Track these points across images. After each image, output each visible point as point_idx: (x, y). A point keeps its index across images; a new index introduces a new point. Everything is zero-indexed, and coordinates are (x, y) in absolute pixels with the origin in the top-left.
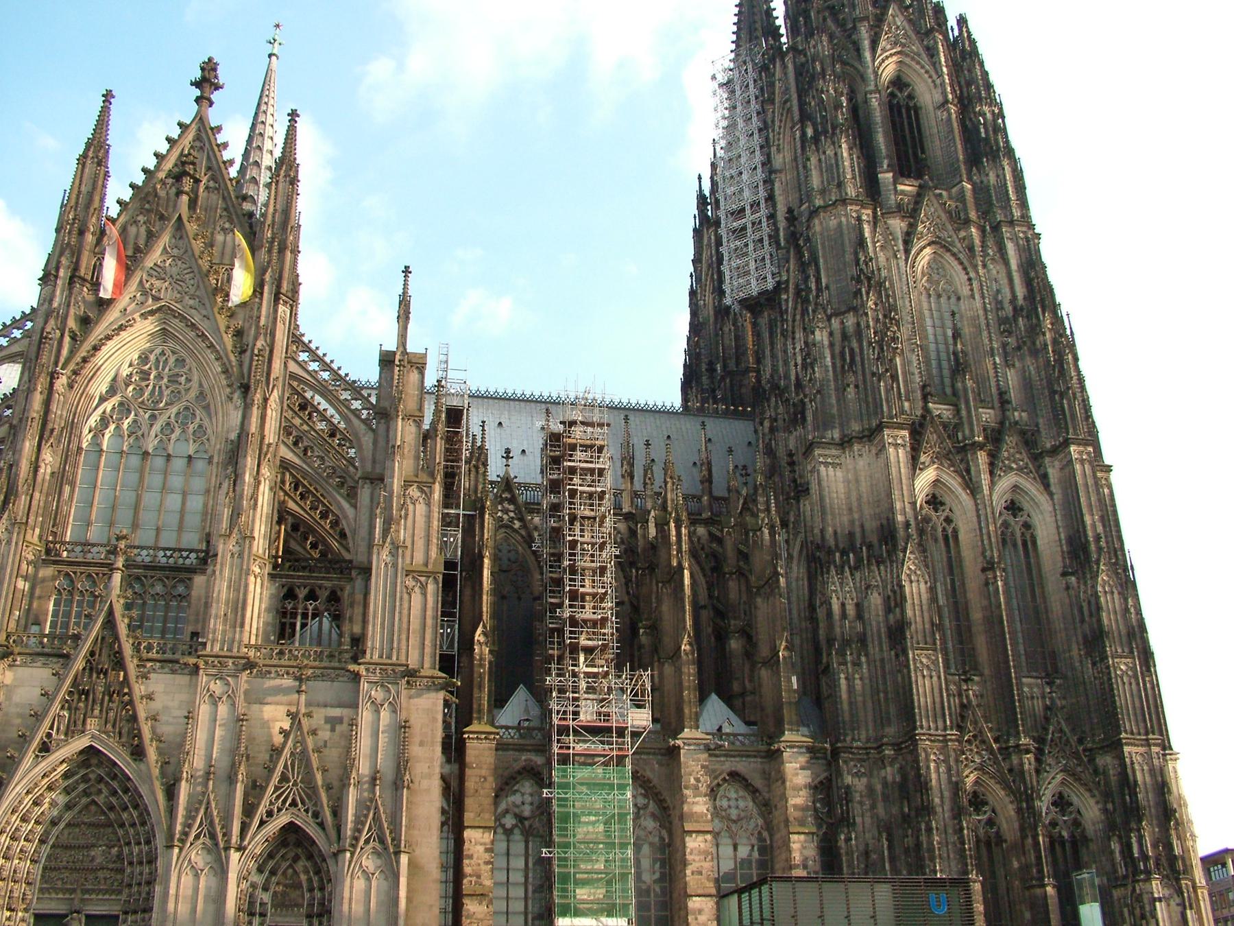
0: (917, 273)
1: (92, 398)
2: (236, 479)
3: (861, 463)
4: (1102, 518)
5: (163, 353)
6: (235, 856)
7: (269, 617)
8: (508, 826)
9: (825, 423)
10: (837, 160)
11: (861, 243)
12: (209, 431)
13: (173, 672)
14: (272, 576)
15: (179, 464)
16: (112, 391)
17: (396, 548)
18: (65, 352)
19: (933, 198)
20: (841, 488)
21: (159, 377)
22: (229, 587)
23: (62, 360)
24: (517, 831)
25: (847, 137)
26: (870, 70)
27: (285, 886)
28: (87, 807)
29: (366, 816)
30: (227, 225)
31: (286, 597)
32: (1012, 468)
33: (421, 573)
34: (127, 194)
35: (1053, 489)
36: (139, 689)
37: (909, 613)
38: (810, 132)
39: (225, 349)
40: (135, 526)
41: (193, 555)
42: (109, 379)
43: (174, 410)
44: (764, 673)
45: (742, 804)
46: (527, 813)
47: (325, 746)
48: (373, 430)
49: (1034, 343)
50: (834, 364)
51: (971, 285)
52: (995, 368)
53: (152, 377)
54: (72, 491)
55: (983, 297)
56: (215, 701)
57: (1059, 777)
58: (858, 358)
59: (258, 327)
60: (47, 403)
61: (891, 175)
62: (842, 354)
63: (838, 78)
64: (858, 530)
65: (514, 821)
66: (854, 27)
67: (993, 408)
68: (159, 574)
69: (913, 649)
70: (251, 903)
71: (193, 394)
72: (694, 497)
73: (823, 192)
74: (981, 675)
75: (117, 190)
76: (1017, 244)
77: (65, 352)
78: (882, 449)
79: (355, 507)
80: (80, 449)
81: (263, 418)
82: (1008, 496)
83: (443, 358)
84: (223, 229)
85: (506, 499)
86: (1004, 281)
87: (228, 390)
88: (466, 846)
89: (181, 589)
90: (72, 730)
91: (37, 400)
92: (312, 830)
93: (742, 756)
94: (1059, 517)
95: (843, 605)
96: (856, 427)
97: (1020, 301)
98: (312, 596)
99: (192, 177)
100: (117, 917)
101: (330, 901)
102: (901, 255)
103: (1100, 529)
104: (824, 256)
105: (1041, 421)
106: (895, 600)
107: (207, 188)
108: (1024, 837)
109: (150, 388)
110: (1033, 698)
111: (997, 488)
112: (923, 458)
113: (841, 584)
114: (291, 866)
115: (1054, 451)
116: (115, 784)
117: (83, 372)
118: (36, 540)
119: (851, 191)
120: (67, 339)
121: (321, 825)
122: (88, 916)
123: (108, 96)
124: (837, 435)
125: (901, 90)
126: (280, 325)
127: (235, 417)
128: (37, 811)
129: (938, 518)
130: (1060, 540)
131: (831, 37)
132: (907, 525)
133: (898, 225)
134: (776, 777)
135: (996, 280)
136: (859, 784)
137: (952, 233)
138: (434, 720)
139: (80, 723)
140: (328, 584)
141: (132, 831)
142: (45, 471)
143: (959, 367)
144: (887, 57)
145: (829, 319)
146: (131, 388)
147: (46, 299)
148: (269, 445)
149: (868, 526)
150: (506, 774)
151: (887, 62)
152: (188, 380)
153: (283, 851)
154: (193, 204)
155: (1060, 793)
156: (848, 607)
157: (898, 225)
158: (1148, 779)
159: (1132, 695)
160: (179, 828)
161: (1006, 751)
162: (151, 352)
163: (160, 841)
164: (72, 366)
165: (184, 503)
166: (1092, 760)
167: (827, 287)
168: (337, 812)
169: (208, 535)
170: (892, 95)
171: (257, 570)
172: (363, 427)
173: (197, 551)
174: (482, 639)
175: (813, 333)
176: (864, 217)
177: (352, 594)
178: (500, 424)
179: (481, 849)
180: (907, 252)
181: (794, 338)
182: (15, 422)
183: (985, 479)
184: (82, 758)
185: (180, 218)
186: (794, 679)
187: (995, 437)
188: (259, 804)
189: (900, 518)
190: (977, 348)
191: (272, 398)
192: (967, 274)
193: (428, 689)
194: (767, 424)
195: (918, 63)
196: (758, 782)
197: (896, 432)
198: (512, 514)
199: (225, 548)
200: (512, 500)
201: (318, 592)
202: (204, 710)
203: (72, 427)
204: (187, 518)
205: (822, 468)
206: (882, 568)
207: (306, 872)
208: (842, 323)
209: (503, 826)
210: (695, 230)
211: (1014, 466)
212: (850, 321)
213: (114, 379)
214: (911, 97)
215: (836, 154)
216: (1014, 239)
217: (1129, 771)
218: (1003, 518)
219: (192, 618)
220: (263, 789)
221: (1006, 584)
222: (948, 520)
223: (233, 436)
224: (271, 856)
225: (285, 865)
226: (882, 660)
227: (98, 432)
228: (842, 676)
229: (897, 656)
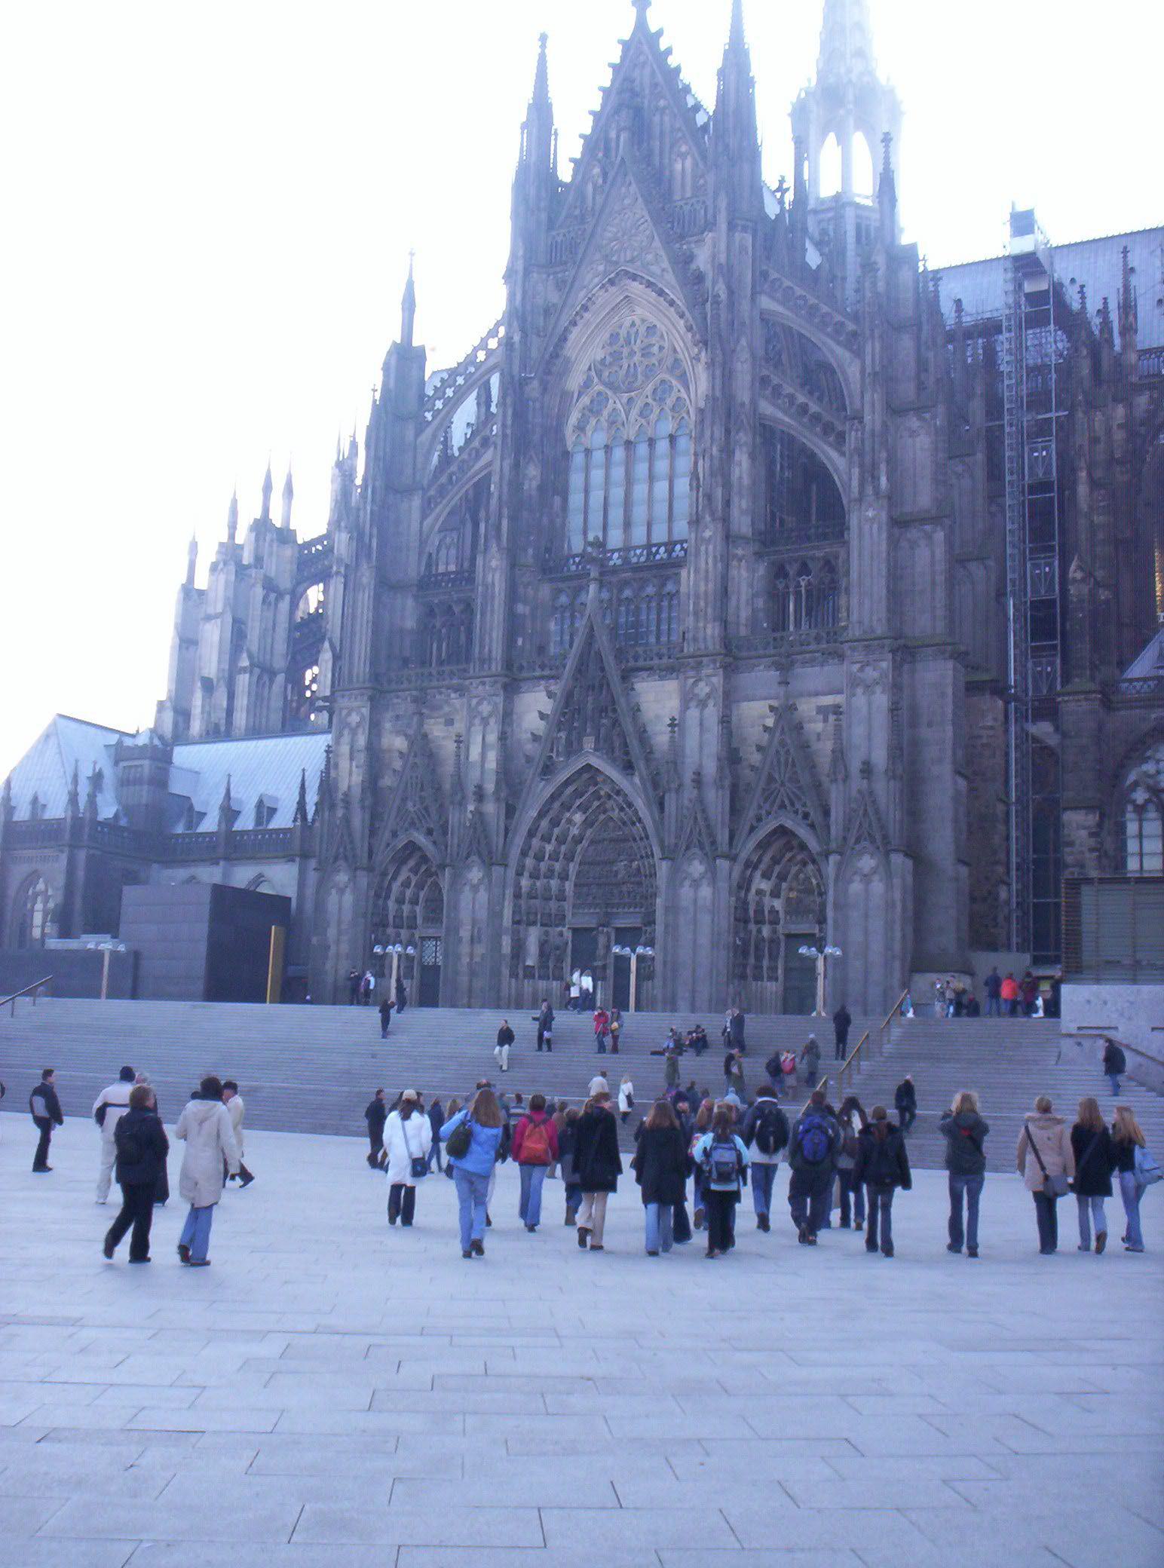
5: (633, 324)
6: (723, 864)
7: (760, 603)
8: (1140, 801)
13: (661, 678)
14: (759, 555)
15: (663, 446)
24: (1151, 807)
27: (799, 891)
28: (605, 823)
30: (684, 149)
31: (777, 576)
40: (627, 525)
47: (819, 739)
65: (1146, 796)
68: (645, 575)
71: (669, 362)
80: (567, 455)
88: (1066, 832)
89: (670, 587)
90: (573, 749)
92: (803, 832)
98: (804, 569)
100: (640, 929)
109: (625, 366)
114: (800, 871)
116: (620, 799)
117: (554, 369)
118: (530, 561)
121: (812, 826)
122: (617, 929)
128: (556, 831)
138: (943, 695)
141: (641, 844)
148: (743, 404)
152: (661, 348)
153: (788, 855)
163: (657, 850)
168: (826, 813)
174: (1079, 575)
179: (1084, 833)
184: (586, 776)
201: (811, 565)
204: (676, 505)
213: (590, 369)
224: (775, 861)
225: (794, 869)
227: (580, 428)
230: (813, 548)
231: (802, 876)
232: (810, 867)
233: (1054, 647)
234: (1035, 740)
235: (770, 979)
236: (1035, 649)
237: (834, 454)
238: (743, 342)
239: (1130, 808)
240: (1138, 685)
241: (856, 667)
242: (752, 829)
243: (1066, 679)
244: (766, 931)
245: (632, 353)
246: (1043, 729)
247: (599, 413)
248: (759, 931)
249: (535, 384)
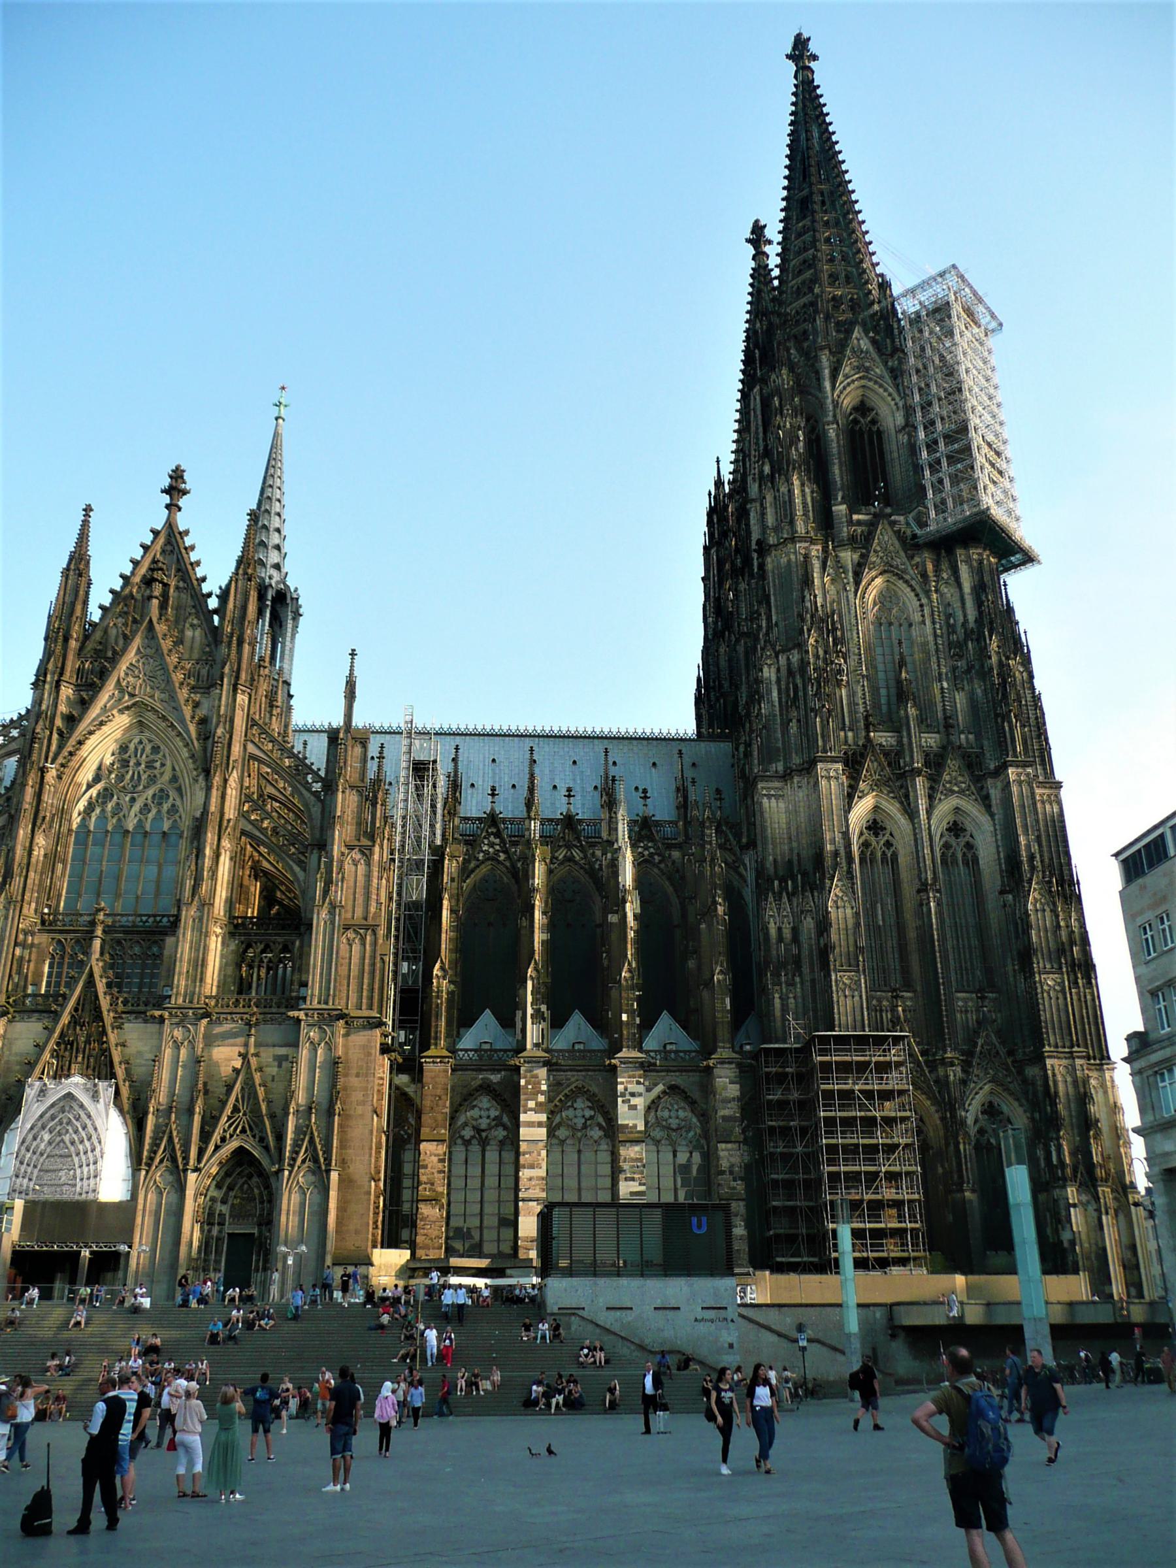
0: (864, 601)
1: (80, 785)
2: (200, 853)
3: (801, 794)
4: (1038, 839)
5: (141, 742)
7: (230, 970)
8: (467, 1137)
9: (769, 756)
10: (790, 497)
11: (807, 581)
12: (181, 809)
13: (146, 1021)
14: (232, 935)
15: (157, 838)
16: (97, 779)
17: (333, 907)
18: (54, 748)
19: (887, 526)
20: (783, 818)
21: (138, 764)
22: (191, 948)
23: (51, 755)
24: (474, 1142)
25: (799, 474)
26: (829, 400)
29: (303, 1140)
30: (195, 622)
32: (953, 792)
33: (361, 927)
34: (107, 600)
35: (994, 809)
36: (113, 1037)
37: (834, 937)
38: (767, 469)
39: (190, 737)
41: (165, 920)
42: (95, 767)
43: (150, 792)
44: (705, 994)
45: (681, 1114)
46: (483, 1126)
48: (321, 801)
49: (982, 666)
50: (780, 699)
52: (942, 692)
53: (131, 764)
54: (64, 868)
55: (934, 623)
56: (177, 1046)
57: (987, 1088)
58: (801, 694)
59: (219, 716)
60: (39, 795)
61: (843, 507)
62: (788, 689)
63: (796, 412)
64: (795, 858)
65: (472, 1133)
66: (816, 356)
67: (938, 732)
68: (136, 937)
69: (835, 971)
70: (211, 1214)
72: (671, 822)
73: (777, 529)
74: (914, 991)
75: (99, 597)
76: (971, 567)
77: (54, 748)
78: (816, 783)
79: (305, 870)
80: (70, 830)
81: (223, 797)
82: (951, 818)
83: (408, 718)
84: (192, 625)
85: (492, 833)
86: (957, 604)
87: (195, 773)
88: (422, 1157)
91: (29, 792)
93: (681, 1071)
94: (999, 837)
95: (780, 929)
96: (796, 760)
97: (971, 623)
99: (161, 582)
101: (270, 1213)
102: (851, 588)
103: (1035, 848)
104: (775, 594)
105: (985, 743)
106: (823, 925)
107: (177, 588)
108: (947, 1145)
109: (131, 773)
110: (966, 1011)
111: (937, 813)
112: (862, 786)
113: (779, 909)
117: (71, 764)
119: (800, 527)
120: (55, 736)
121: (267, 1148)
123: (88, 510)
124: (780, 767)
125: (864, 415)
126: (238, 712)
127: (200, 797)
128: (35, 1143)
129: (878, 844)
130: (999, 859)
131: (791, 369)
132: (836, 854)
133: (848, 557)
134: (707, 1088)
135: (949, 605)
137: (905, 560)
139: (66, 1068)
140: (279, 939)
142: (38, 853)
143: (902, 694)
144: (849, 384)
145: (777, 657)
146: (113, 776)
147: (38, 702)
149: (804, 853)
150: (465, 1091)
151: (849, 389)
152: (163, 765)
154: (163, 606)
155: (990, 1103)
156: (785, 931)
157: (848, 557)
158: (1071, 1090)
159: (1058, 1010)
160: (145, 1153)
161: (932, 1065)
162: (130, 742)
164: (60, 760)
165: (159, 873)
166: (1020, 1072)
167: (776, 624)
168: (280, 1137)
169: (179, 900)
170: (855, 421)
171: (219, 930)
172: (312, 798)
173: (168, 916)
175: (761, 670)
176: (814, 553)
178: (494, 760)
179: (435, 1159)
180: (857, 583)
182: (13, 812)
183: (922, 804)
185: (151, 621)
186: (728, 1000)
187: (935, 763)
188: (214, 1131)
189: (829, 847)
190: (926, 673)
191: (231, 779)
193: (364, 1028)
194: (742, 749)
195: (881, 386)
196: (696, 1095)
197: (829, 765)
198: (498, 847)
199: (189, 914)
200: (498, 835)
202: (168, 1053)
203: (63, 813)
205: (765, 800)
206: (816, 894)
207: (258, 1188)
208: (788, 659)
209: (462, 1137)
210: (705, 548)
211: (956, 789)
212: (795, 657)
213: (99, 768)
214: (874, 422)
215: (789, 491)
216: (968, 561)
217: (1051, 1083)
218: (944, 839)
219: (164, 974)
220: (216, 1119)
221: (938, 904)
222: (888, 844)
223: (198, 814)
224: (228, 1174)
225: (241, 1181)
228: (777, 995)
230: (276, 935)
231: (246, 1186)
232: (255, 1179)
233: (416, 1022)
234: (397, 1088)
235: (215, 1270)
236: (401, 1021)
237: (297, 869)
238: (235, 774)
239: (459, 1141)
240: (471, 1054)
242: (217, 1148)
243: (425, 1046)
244: (215, 1232)
245: (138, 764)
246: (403, 1079)
247: (104, 803)
248: (209, 1231)
249: (54, 773)
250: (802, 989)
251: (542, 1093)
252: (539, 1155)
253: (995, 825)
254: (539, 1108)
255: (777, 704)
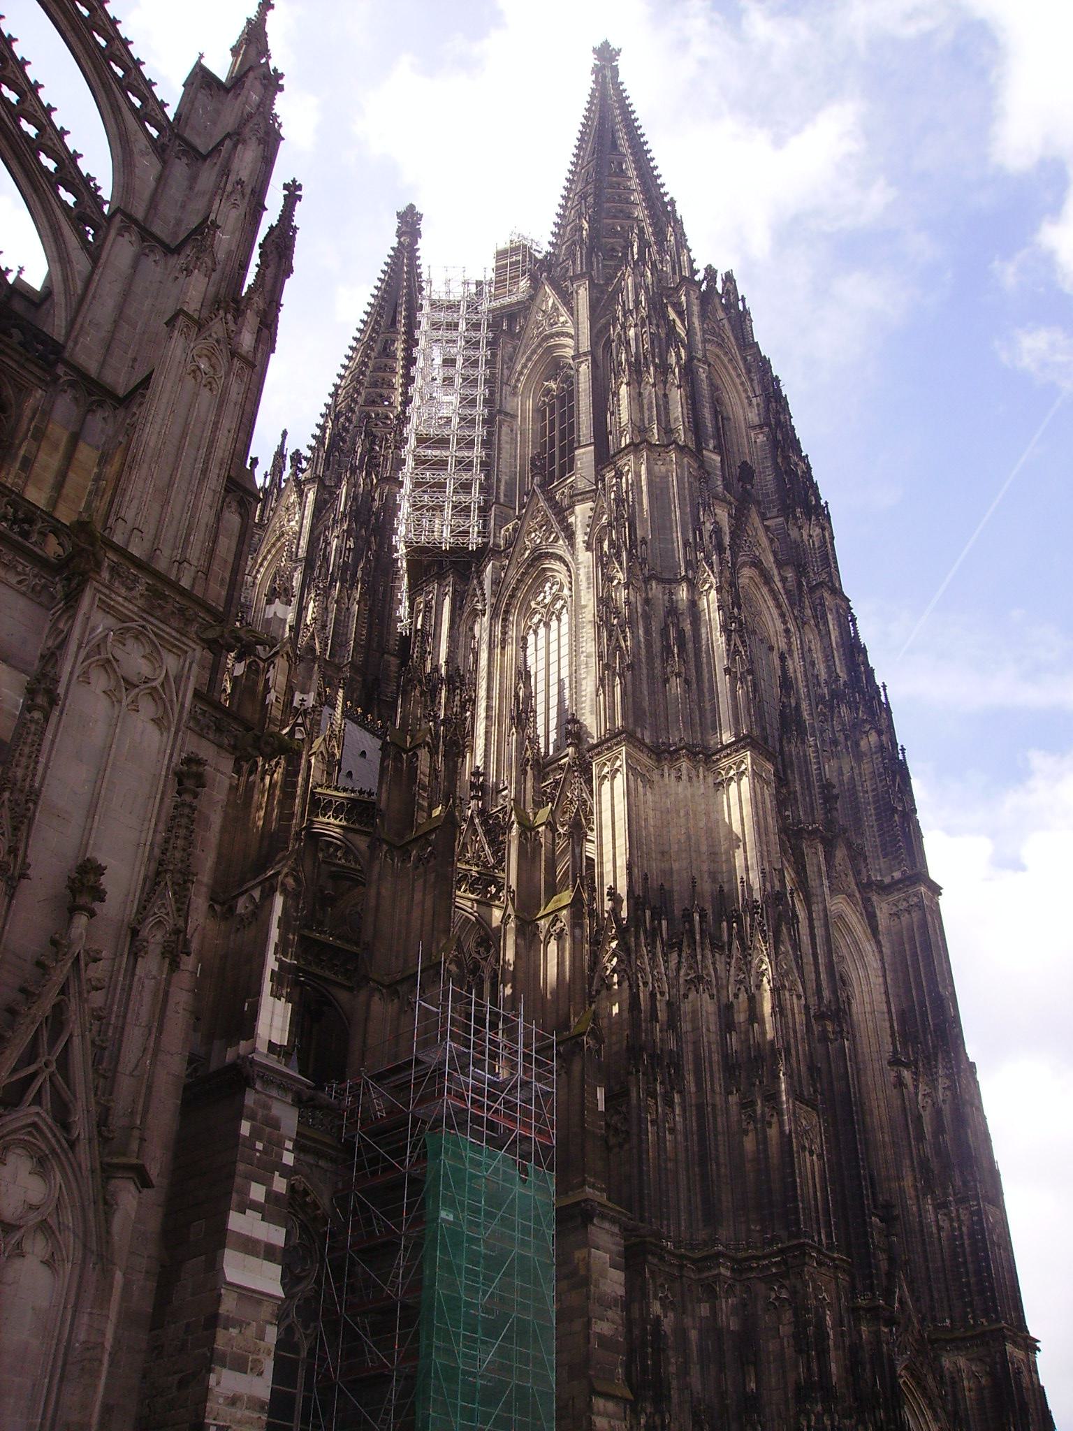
51: (789, 638)
115: (884, 889)
136: (668, 1324)
145: (647, 581)
177: (45, 413)
181: (505, 620)
186: (600, 1094)
192: (785, 622)
226: (714, 1106)
229: (747, 1104)
241: (102, 623)
250: (685, 1119)
251: (286, 1172)
252: (261, 1337)
253: (882, 960)
254: (271, 1210)
255: (643, 646)
